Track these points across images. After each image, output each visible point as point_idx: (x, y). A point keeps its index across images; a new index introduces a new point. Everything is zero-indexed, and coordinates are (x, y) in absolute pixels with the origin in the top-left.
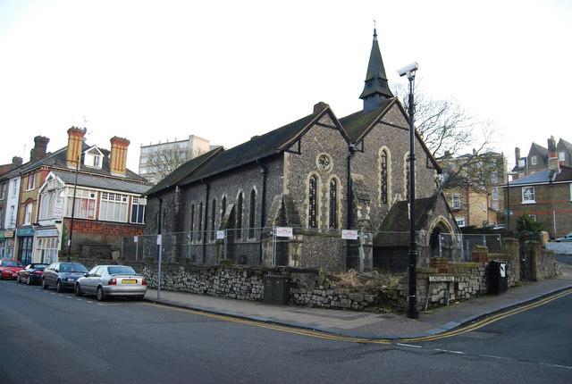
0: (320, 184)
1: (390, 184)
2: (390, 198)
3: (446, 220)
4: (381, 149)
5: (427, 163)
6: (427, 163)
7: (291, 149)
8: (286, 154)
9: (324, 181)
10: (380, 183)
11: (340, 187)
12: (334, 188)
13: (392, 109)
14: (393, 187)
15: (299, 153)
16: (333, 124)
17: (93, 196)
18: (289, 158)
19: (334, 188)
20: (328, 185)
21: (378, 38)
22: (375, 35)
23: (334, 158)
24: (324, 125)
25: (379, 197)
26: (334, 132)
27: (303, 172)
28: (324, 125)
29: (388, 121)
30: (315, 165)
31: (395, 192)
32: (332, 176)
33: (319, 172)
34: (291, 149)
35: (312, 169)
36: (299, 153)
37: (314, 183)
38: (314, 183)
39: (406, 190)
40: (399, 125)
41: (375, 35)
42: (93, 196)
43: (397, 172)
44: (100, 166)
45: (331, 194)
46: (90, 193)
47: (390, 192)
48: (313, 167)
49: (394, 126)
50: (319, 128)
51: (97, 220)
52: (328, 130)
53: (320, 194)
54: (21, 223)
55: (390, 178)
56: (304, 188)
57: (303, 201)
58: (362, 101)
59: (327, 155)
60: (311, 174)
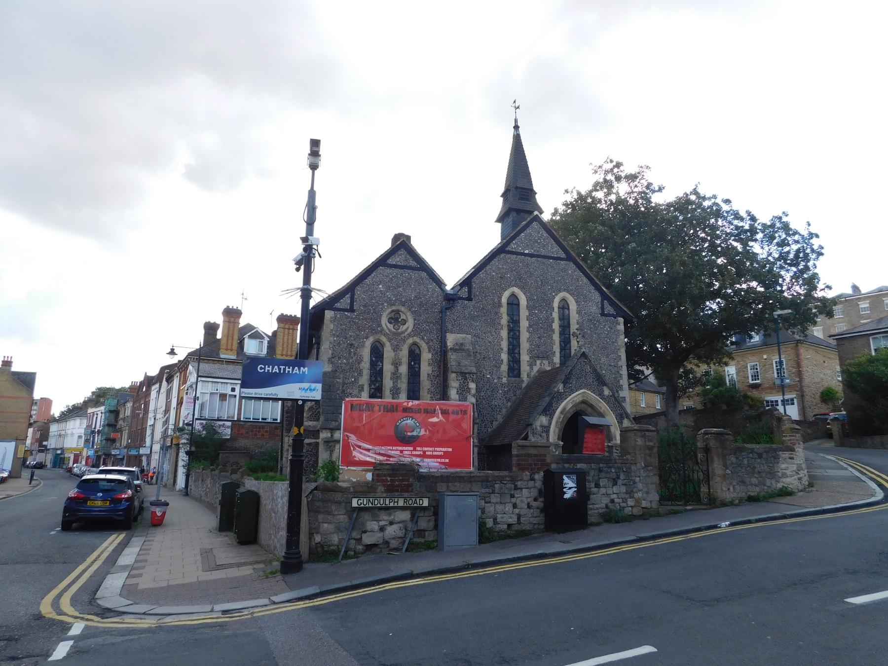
0: (388, 353)
1: (524, 344)
2: (525, 368)
3: (592, 397)
4: (506, 295)
5: (603, 308)
6: (603, 308)
7: (338, 305)
8: (329, 314)
9: (396, 348)
10: (505, 345)
11: (426, 356)
12: (414, 356)
13: (528, 231)
14: (530, 351)
15: (352, 310)
16: (413, 263)
17: (233, 390)
18: (334, 319)
19: (414, 356)
20: (404, 353)
21: (521, 131)
22: (516, 127)
23: (414, 313)
25: (504, 368)
26: (414, 275)
27: (357, 337)
29: (520, 250)
30: (380, 325)
32: (410, 341)
33: (385, 335)
34: (338, 305)
35: (374, 331)
36: (352, 310)
37: (377, 353)
38: (377, 353)
39: (558, 354)
40: (543, 252)
41: (516, 127)
42: (233, 390)
43: (540, 327)
44: (265, 351)
45: (410, 367)
46: (229, 387)
47: (525, 358)
48: (376, 329)
49: (531, 255)
50: (388, 271)
51: (239, 420)
52: (407, 273)
53: (388, 368)
54: (177, 424)
55: (524, 336)
56: (360, 361)
57: (356, 380)
58: (499, 225)
59: (403, 309)
60: (371, 339)
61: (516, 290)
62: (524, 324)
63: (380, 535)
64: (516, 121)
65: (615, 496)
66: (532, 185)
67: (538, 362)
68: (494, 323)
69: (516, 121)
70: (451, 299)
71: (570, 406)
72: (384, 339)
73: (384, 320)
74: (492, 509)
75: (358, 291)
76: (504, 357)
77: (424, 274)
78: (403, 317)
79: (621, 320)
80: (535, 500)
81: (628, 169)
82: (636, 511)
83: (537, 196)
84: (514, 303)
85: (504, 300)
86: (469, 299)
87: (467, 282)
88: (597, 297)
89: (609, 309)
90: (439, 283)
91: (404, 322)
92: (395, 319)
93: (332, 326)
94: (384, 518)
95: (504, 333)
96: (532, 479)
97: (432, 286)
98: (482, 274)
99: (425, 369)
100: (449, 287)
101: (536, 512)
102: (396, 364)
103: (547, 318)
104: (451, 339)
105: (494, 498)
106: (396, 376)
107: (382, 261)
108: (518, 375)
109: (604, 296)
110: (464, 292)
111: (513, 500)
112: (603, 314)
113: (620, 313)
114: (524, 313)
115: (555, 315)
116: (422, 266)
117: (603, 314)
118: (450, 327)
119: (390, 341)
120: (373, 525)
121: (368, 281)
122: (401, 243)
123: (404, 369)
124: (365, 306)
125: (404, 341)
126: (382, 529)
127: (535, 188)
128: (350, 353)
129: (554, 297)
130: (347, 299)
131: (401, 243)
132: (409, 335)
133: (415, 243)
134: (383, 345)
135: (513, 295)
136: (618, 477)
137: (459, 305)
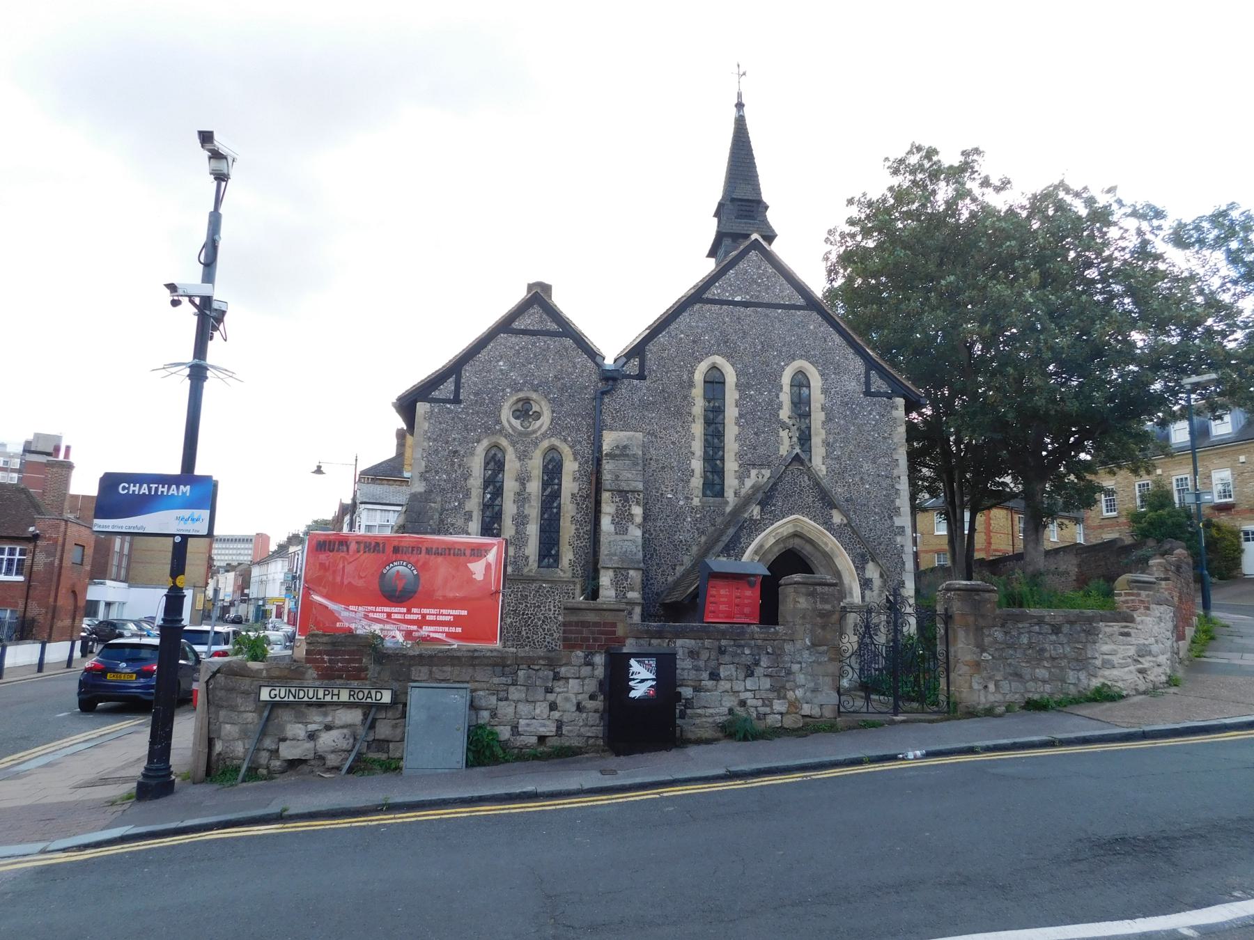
2: (731, 482)
3: (810, 525)
5: (868, 383)
7: (435, 394)
9: (523, 456)
10: (698, 446)
11: (570, 467)
12: (552, 471)
13: (742, 265)
14: (740, 456)
15: (456, 400)
16: (553, 326)
18: (429, 416)
19: (552, 471)
20: (536, 464)
21: (747, 112)
22: (740, 106)
23: (552, 401)
24: (525, 332)
25: (697, 482)
26: (553, 343)
27: (464, 441)
28: (525, 332)
29: (727, 296)
30: (499, 422)
31: (746, 466)
32: (545, 444)
35: (488, 431)
36: (456, 400)
37: (495, 463)
38: (495, 463)
40: (766, 298)
41: (740, 106)
47: (731, 466)
48: (492, 427)
49: (745, 304)
50: (514, 339)
52: (541, 342)
53: (510, 486)
55: (731, 431)
59: (534, 396)
60: (485, 443)
61: (719, 360)
62: (731, 412)
63: (310, 745)
64: (740, 95)
65: (749, 695)
66: (759, 194)
67: (754, 472)
68: (681, 414)
69: (740, 95)
70: (611, 379)
71: (772, 541)
72: (504, 442)
73: (506, 414)
74: (511, 710)
75: (467, 372)
76: (697, 465)
77: (569, 342)
78: (535, 408)
79: (900, 401)
80: (592, 697)
81: (949, 158)
82: (789, 722)
83: (770, 215)
84: (715, 383)
85: (699, 376)
86: (641, 376)
87: (637, 351)
88: (858, 365)
89: (878, 384)
90: (593, 355)
91: (538, 416)
92: (524, 411)
93: (426, 426)
94: (316, 720)
95: (698, 429)
96: (589, 664)
97: (582, 358)
98: (662, 338)
99: (569, 486)
100: (609, 361)
101: (594, 718)
102: (522, 480)
103: (771, 402)
104: (609, 440)
105: (515, 693)
106: (521, 497)
107: (505, 326)
108: (721, 493)
109: (870, 364)
110: (633, 366)
111: (551, 697)
112: (868, 393)
113: (898, 389)
114: (731, 395)
115: (785, 397)
116: (566, 330)
117: (868, 393)
118: (609, 421)
119: (513, 444)
120: (296, 730)
121: (483, 355)
122: (539, 297)
123: (534, 487)
124: (476, 394)
125: (536, 445)
126: (312, 736)
127: (765, 197)
128: (453, 464)
129: (783, 369)
130: (450, 385)
131: (539, 297)
132: (544, 436)
133: (560, 300)
134: (503, 451)
135: (800, 372)
136: (757, 664)
137: (624, 388)
